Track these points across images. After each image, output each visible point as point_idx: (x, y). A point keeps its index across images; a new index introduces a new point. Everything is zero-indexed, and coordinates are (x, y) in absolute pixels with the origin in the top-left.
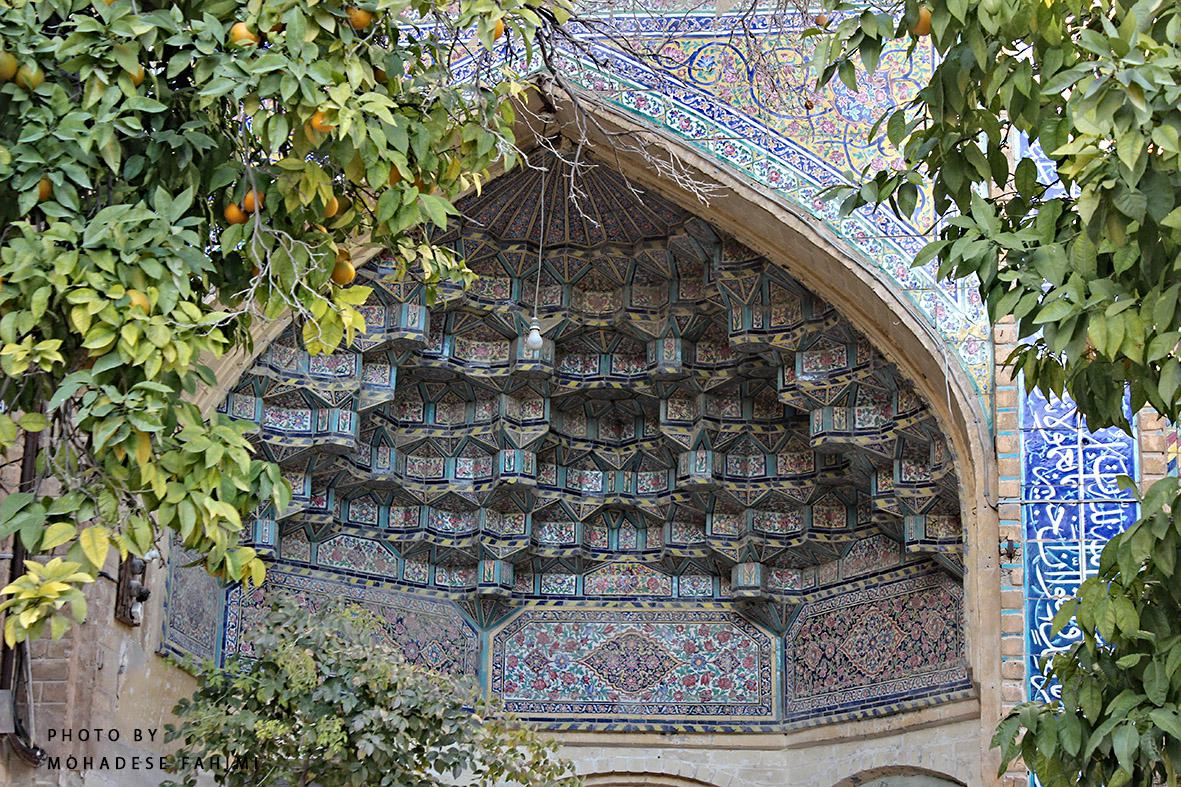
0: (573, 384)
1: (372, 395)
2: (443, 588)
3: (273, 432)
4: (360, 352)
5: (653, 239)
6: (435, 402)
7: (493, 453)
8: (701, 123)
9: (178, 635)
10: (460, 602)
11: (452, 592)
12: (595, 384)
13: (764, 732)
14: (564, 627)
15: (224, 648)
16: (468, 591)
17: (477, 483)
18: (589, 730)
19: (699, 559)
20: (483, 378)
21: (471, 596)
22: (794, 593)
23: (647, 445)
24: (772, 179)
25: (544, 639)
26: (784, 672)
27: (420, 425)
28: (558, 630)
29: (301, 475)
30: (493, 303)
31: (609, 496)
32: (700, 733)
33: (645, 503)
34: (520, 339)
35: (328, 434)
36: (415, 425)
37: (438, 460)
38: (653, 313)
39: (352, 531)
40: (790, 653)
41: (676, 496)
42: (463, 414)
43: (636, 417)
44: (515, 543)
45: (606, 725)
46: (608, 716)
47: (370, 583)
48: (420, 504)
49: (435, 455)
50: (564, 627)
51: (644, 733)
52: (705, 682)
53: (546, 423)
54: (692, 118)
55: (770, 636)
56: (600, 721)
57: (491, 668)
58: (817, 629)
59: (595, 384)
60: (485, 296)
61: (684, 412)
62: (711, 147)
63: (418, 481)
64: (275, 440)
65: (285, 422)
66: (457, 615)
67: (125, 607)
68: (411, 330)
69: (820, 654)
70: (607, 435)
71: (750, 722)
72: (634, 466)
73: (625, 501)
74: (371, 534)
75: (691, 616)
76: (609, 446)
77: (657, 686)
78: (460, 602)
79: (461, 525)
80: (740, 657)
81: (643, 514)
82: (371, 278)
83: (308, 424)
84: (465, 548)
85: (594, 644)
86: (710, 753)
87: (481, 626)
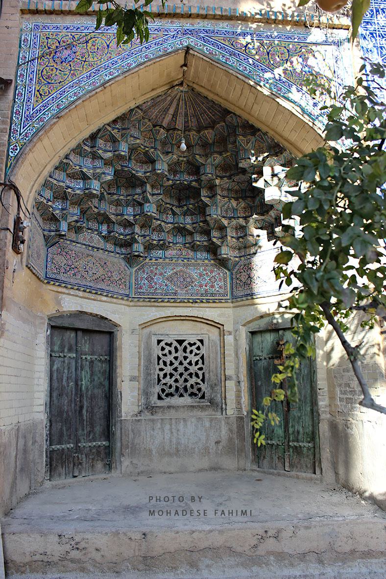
0: (171, 182)
1: (105, 176)
2: (118, 253)
3: (69, 187)
4: (103, 159)
5: (208, 127)
6: (121, 186)
7: (141, 205)
8: (251, 69)
9: (33, 261)
10: (123, 258)
11: (121, 255)
12: (178, 182)
13: (226, 302)
14: (158, 267)
15: (46, 269)
16: (127, 254)
17: (135, 216)
18: (168, 302)
19: (205, 246)
20: (141, 176)
21: (129, 256)
22: (237, 257)
23: (191, 206)
24: (278, 90)
25: (152, 271)
26: (232, 284)
27: (116, 194)
28: (156, 269)
29: (76, 206)
30: (148, 148)
31: (176, 223)
32: (205, 303)
33: (188, 226)
34: (157, 162)
35: (90, 189)
36: (114, 194)
37: (120, 207)
38: (203, 156)
39: (89, 231)
40: (234, 277)
41: (200, 223)
42: (130, 191)
43: (186, 197)
44: (145, 238)
45: (174, 300)
46: (174, 297)
47: (95, 250)
48: (114, 223)
49: (120, 206)
50: (158, 267)
51: (186, 302)
52: (206, 286)
53: (161, 194)
54: (247, 67)
55: (227, 271)
56: (172, 299)
57: (134, 281)
58: (246, 268)
59: (178, 182)
60: (146, 145)
61: (209, 193)
62: (255, 78)
63: (114, 214)
64: (69, 190)
65: (73, 184)
66: (123, 263)
67: (16, 244)
68: (123, 152)
69: (247, 277)
70: (176, 203)
71: (222, 299)
72: (185, 214)
73: (181, 225)
74: (96, 233)
75: (201, 265)
76: (177, 207)
77: (190, 287)
78: (123, 258)
79: (126, 231)
80: (218, 278)
81: (187, 230)
82: (110, 130)
83: (82, 185)
84: (128, 239)
85: (169, 273)
86: (207, 309)
87: (131, 267)
